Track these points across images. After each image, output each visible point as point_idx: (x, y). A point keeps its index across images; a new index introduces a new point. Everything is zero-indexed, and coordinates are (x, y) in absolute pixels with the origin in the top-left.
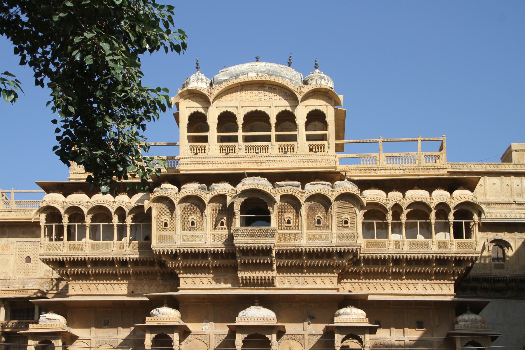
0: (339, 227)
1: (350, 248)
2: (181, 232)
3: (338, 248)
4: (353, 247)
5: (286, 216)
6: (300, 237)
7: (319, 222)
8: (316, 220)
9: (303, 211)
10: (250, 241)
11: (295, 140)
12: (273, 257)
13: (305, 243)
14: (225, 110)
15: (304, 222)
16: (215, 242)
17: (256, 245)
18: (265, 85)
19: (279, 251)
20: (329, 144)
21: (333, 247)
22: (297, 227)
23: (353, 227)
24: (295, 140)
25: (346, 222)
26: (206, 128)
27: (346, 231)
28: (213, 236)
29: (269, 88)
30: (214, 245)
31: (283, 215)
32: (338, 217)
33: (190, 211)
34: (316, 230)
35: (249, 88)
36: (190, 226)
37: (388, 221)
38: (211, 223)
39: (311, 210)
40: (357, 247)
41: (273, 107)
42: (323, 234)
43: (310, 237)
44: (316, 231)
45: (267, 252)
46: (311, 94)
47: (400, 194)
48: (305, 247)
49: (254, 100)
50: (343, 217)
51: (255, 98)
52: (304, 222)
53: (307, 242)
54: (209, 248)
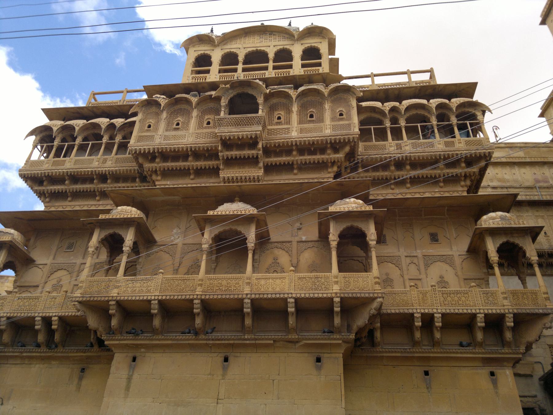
0: (333, 119)
1: (346, 137)
2: (163, 132)
3: (333, 138)
4: (350, 136)
5: (276, 114)
6: (290, 131)
7: (311, 116)
8: (309, 115)
9: (295, 108)
10: (234, 130)
11: (292, 68)
12: (259, 150)
13: (296, 134)
14: (229, 50)
15: (295, 117)
16: (198, 139)
17: (240, 133)
18: (267, 33)
19: (266, 146)
20: (323, 69)
21: (327, 138)
22: (288, 122)
23: (349, 118)
24: (292, 68)
25: (341, 115)
26: (210, 64)
27: (341, 123)
28: (197, 134)
29: (269, 34)
30: (196, 142)
31: (274, 113)
32: (333, 110)
33: (177, 114)
34: (309, 123)
35: (252, 36)
36: (175, 126)
37: (386, 125)
38: (197, 124)
39: (303, 107)
40: (354, 136)
41: (272, 47)
42: (316, 126)
43: (302, 131)
44: (308, 125)
45: (252, 143)
46: (307, 35)
47: (398, 103)
48: (295, 139)
49: (255, 43)
50: (338, 111)
51: (257, 41)
52: (295, 117)
53: (298, 134)
54: (190, 145)
